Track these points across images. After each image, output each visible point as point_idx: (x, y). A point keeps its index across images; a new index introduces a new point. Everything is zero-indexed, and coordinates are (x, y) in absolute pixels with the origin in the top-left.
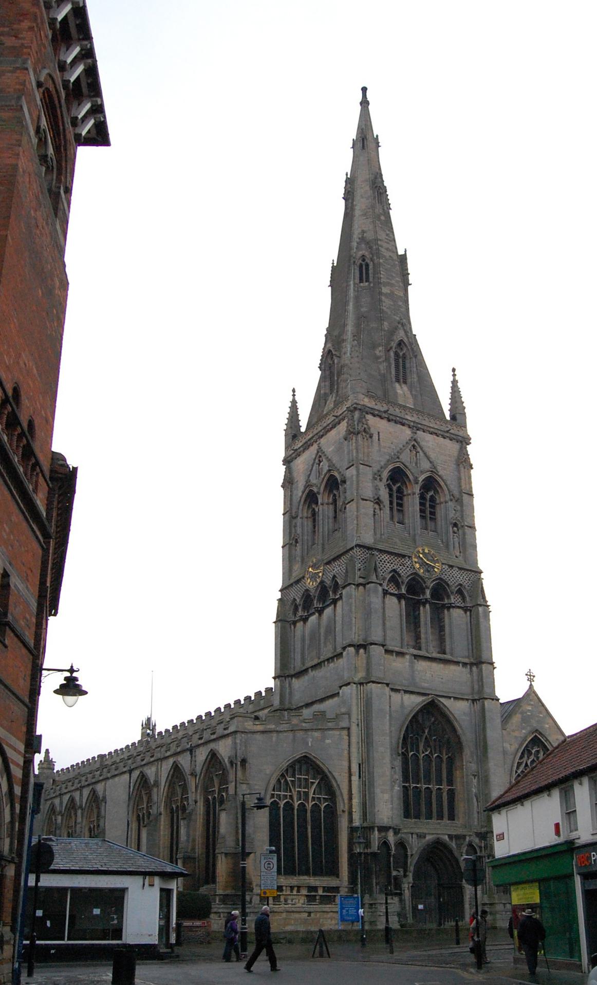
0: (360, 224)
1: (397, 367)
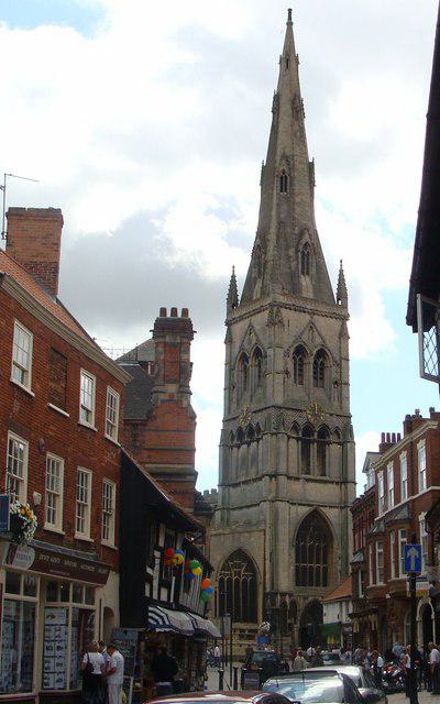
0: (283, 138)
1: (303, 266)
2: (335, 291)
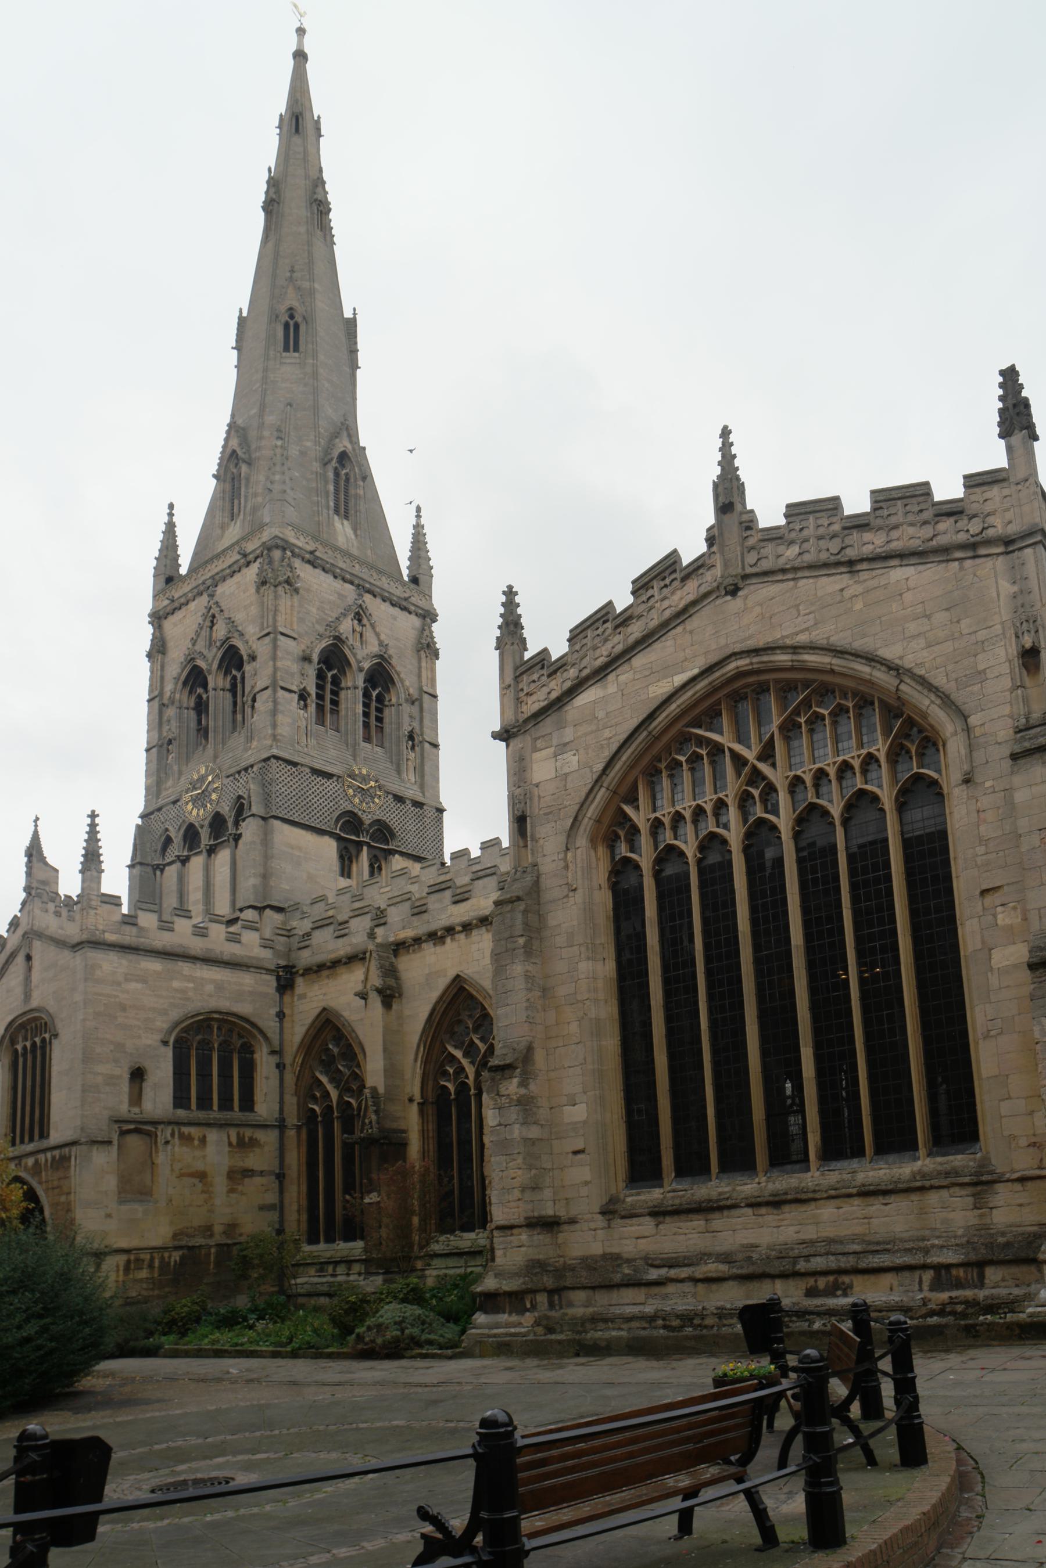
2: (404, 563)
